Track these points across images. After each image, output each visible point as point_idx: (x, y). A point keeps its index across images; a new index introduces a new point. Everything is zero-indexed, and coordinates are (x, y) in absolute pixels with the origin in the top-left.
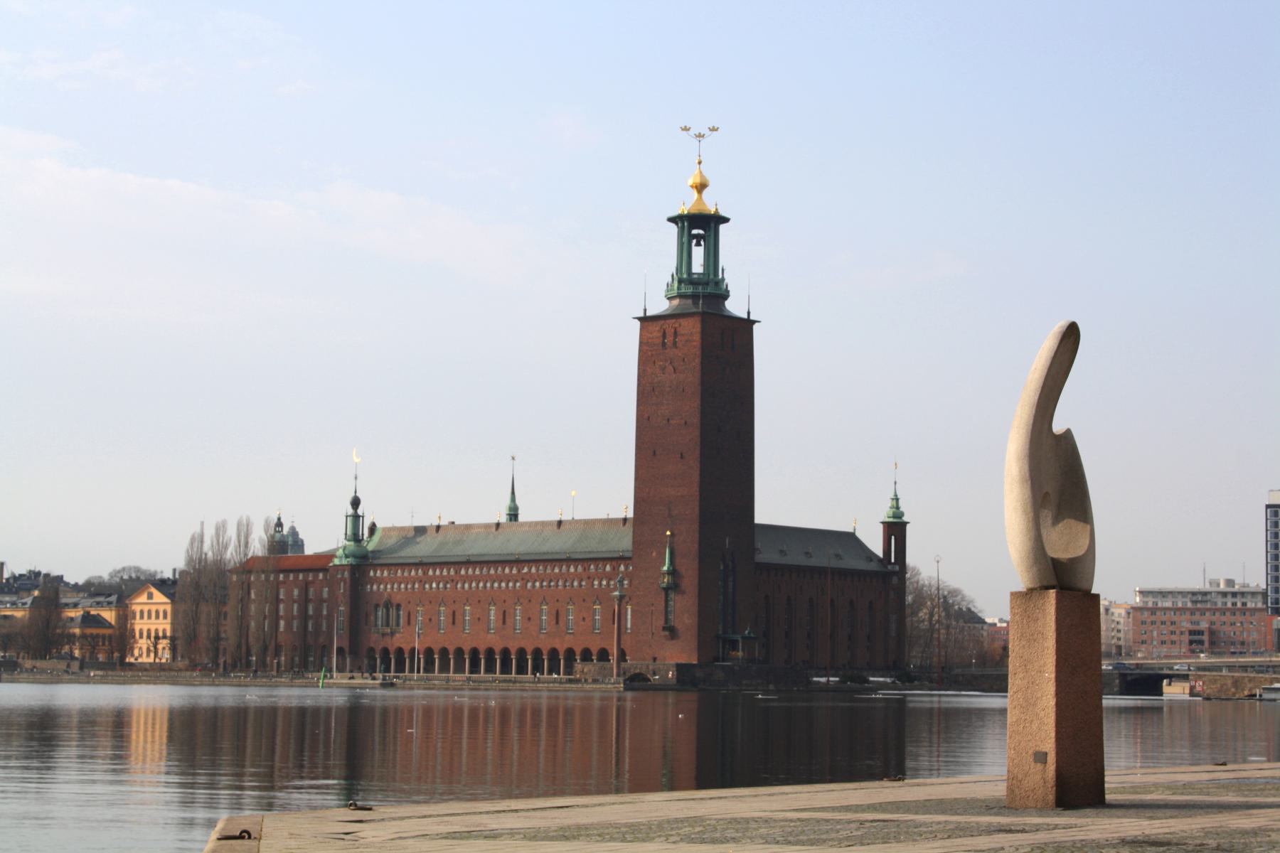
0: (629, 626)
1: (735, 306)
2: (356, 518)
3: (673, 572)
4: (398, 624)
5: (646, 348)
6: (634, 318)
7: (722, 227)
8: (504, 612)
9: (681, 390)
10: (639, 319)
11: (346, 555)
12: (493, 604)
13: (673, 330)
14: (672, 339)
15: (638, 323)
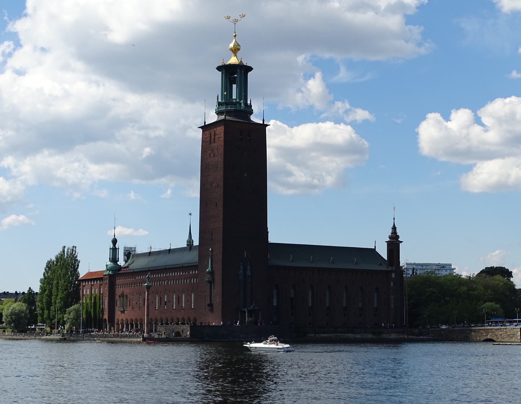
0: (183, 305)
1: (255, 119)
2: (114, 250)
3: (212, 273)
4: (127, 306)
5: (204, 144)
6: (199, 128)
7: (250, 74)
8: (161, 298)
9: (216, 166)
10: (201, 127)
11: (107, 269)
12: (157, 294)
13: (214, 133)
14: (213, 137)
15: (201, 130)
